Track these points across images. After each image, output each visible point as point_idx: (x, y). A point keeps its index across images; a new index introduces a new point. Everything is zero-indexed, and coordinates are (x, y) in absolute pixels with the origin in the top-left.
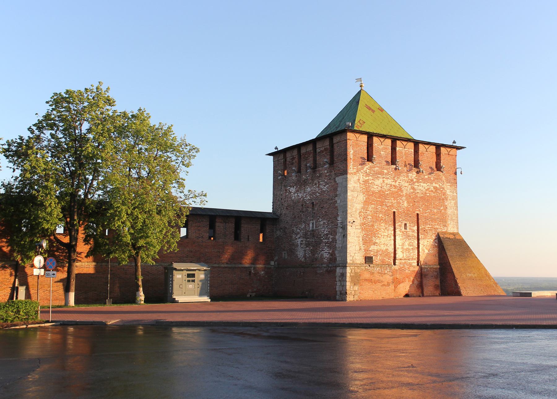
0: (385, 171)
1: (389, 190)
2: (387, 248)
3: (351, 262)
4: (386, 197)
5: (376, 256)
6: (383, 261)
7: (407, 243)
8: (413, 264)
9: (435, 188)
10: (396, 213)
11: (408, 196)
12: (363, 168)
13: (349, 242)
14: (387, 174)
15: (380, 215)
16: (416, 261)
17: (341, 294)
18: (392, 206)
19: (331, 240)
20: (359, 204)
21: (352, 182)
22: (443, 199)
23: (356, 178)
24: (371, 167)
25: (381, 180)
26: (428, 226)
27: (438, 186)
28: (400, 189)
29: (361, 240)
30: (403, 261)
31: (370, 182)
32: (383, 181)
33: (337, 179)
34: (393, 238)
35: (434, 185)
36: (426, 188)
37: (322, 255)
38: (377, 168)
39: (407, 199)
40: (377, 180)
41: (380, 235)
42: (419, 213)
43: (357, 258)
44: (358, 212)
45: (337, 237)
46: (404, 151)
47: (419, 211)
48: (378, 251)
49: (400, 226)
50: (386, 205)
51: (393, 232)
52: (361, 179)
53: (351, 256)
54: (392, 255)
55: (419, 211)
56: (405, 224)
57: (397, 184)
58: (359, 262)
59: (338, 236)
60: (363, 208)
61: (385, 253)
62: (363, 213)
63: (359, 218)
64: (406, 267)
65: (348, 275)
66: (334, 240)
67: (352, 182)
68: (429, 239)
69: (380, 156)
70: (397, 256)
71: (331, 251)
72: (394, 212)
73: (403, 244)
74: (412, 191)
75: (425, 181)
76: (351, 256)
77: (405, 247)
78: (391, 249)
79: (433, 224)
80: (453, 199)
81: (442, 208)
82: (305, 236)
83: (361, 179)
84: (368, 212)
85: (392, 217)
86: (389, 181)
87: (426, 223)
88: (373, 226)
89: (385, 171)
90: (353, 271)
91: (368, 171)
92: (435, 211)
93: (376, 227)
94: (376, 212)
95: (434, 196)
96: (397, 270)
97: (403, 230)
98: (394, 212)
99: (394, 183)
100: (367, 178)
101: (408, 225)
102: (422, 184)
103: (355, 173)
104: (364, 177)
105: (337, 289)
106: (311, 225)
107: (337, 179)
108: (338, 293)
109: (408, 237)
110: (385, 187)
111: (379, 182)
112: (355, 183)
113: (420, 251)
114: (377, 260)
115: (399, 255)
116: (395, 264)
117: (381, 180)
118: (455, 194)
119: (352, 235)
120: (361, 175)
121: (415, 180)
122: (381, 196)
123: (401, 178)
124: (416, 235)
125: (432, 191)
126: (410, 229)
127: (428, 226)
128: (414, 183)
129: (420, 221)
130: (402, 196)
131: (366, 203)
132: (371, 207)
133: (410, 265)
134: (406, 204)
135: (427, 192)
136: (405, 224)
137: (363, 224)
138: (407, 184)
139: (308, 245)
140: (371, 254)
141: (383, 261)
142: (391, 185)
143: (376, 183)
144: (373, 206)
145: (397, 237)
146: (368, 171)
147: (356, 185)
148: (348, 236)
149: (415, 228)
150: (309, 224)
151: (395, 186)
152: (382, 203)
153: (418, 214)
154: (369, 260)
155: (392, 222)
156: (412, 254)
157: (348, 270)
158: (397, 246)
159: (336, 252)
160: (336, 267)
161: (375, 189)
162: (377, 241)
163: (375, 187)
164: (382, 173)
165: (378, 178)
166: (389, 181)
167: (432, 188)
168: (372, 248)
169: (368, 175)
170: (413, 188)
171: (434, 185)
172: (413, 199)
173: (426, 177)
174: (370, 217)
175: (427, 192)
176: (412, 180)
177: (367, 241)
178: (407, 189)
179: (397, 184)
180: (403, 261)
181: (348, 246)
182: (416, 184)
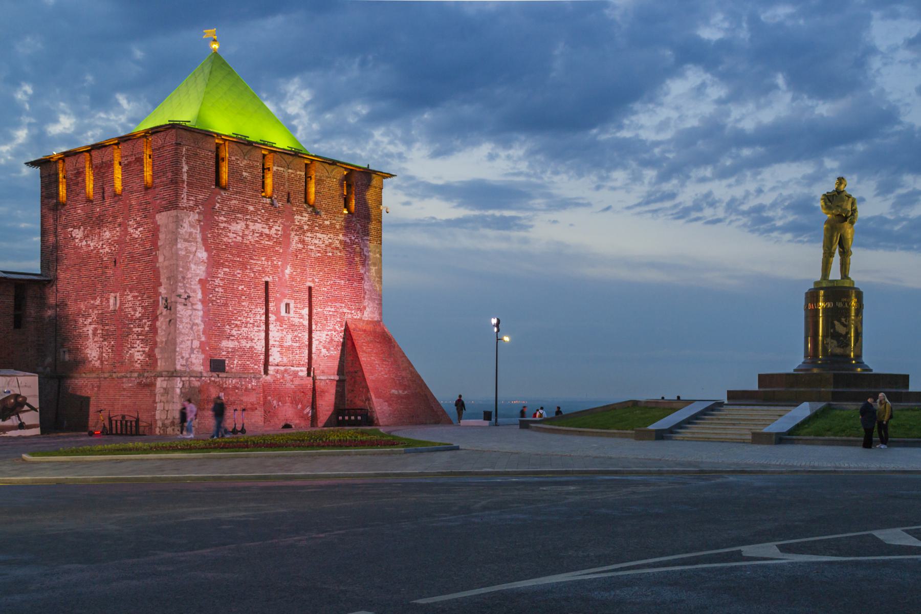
0: (251, 208)
3: (183, 369)
5: (232, 359)
6: (245, 367)
7: (289, 337)
8: (300, 374)
10: (271, 286)
13: (180, 333)
14: (252, 213)
16: (305, 369)
17: (163, 424)
19: (147, 329)
21: (184, 225)
30: (282, 368)
31: (222, 225)
32: (247, 226)
33: (158, 217)
34: (263, 327)
36: (327, 242)
37: (132, 356)
38: (234, 202)
40: (235, 224)
42: (312, 285)
43: (194, 361)
45: (158, 324)
51: (263, 318)
54: (262, 357)
55: (313, 281)
56: (287, 305)
59: (161, 323)
66: (154, 329)
68: (331, 330)
70: (271, 359)
71: (147, 349)
74: (300, 246)
75: (324, 229)
76: (183, 358)
78: (260, 347)
79: (338, 305)
80: (375, 264)
82: (101, 320)
86: (258, 227)
88: (226, 305)
89: (251, 208)
90: (187, 385)
99: (266, 231)
101: (292, 306)
102: (319, 235)
105: (157, 417)
106: (112, 301)
107: (158, 217)
108: (159, 423)
111: (238, 227)
112: (191, 226)
113: (314, 350)
114: (234, 364)
115: (275, 357)
116: (266, 372)
118: (378, 255)
121: (306, 227)
124: (306, 323)
125: (337, 248)
126: (295, 312)
128: (304, 232)
129: (314, 299)
133: (295, 374)
135: (329, 249)
136: (287, 305)
139: (105, 337)
142: (261, 234)
144: (227, 270)
145: (271, 327)
149: (306, 311)
150: (108, 300)
152: (243, 265)
153: (310, 288)
154: (217, 366)
158: (271, 342)
159: (157, 351)
160: (156, 377)
162: (234, 332)
163: (231, 235)
164: (245, 212)
165: (236, 220)
168: (225, 343)
173: (327, 223)
174: (220, 290)
176: (301, 228)
180: (282, 368)
181: (178, 340)
182: (309, 234)
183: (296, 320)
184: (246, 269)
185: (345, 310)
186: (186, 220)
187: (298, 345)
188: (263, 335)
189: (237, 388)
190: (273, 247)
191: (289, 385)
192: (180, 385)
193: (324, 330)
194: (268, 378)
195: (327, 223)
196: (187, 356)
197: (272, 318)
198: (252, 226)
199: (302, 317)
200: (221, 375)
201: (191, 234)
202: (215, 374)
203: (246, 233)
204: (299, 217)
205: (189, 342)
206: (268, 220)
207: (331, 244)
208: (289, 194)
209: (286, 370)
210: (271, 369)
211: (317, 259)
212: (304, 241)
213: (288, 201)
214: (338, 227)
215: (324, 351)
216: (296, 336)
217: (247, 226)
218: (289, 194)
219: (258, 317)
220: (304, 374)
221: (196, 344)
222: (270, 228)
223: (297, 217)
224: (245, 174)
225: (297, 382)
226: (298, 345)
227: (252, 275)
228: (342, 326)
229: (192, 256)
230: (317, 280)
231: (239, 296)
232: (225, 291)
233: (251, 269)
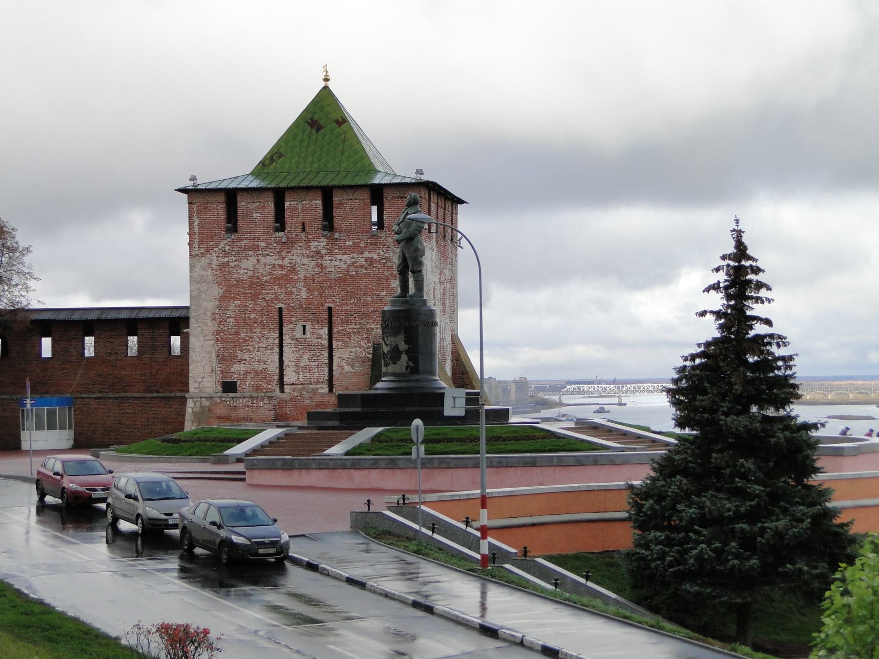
1: (270, 274)
2: (265, 366)
4: (262, 286)
5: (244, 380)
6: (257, 389)
7: (306, 357)
9: (370, 261)
10: (285, 311)
11: (309, 282)
12: (217, 245)
15: (252, 316)
18: (277, 299)
20: (211, 301)
22: (387, 279)
23: (204, 261)
24: (233, 241)
25: (253, 260)
26: (353, 326)
27: (375, 257)
28: (293, 270)
29: (214, 356)
30: (300, 387)
31: (232, 264)
32: (258, 261)
34: (277, 350)
35: (367, 254)
36: (349, 262)
39: (306, 285)
41: (251, 348)
43: (206, 384)
44: (209, 314)
46: (300, 206)
47: (334, 301)
48: (247, 372)
49: (292, 330)
50: (264, 299)
51: (277, 341)
52: (215, 262)
53: (196, 382)
54: (276, 377)
57: (286, 262)
58: (211, 391)
60: (219, 307)
61: (262, 374)
62: (220, 317)
63: (210, 324)
64: (306, 395)
65: (189, 410)
67: (197, 269)
69: (253, 221)
70: (286, 379)
72: (280, 309)
73: (298, 359)
74: (317, 270)
75: (345, 250)
76: (196, 382)
77: (302, 364)
78: (274, 368)
79: (363, 321)
81: (384, 293)
83: (215, 262)
84: (228, 313)
85: (277, 317)
86: (270, 260)
87: (346, 321)
88: (237, 333)
89: (263, 244)
90: (198, 404)
91: (227, 248)
92: (369, 299)
93: (243, 335)
94: (243, 312)
95: (367, 275)
96: (286, 401)
97: (299, 334)
98: (280, 309)
100: (226, 260)
101: (307, 328)
103: (203, 255)
104: (220, 259)
109: (309, 347)
110: (261, 271)
111: (249, 263)
112: (203, 269)
113: (334, 368)
114: (246, 387)
115: (290, 376)
116: (282, 390)
117: (253, 260)
119: (197, 350)
120: (214, 256)
121: (323, 252)
122: (255, 285)
123: (294, 251)
124: (326, 342)
125: (362, 266)
126: (313, 333)
127: (353, 326)
128: (322, 256)
130: (298, 280)
131: (224, 299)
132: (233, 305)
133: (315, 392)
134: (304, 293)
135: (352, 268)
136: (304, 327)
137: (218, 332)
138: (306, 261)
140: (235, 377)
141: (257, 389)
142: (274, 266)
143: (242, 265)
145: (285, 349)
146: (227, 248)
147: (205, 273)
148: (191, 352)
149: (325, 330)
151: (281, 266)
152: (255, 297)
153: (330, 309)
154: (229, 387)
155: (277, 325)
156: (316, 375)
157: (190, 404)
158: (286, 363)
161: (243, 275)
162: (246, 357)
163: (242, 271)
164: (255, 248)
165: (246, 257)
166: (270, 260)
167: (362, 261)
168: (236, 367)
169: (226, 254)
170: (322, 267)
171: (367, 254)
172: (319, 284)
173: (350, 243)
174: (232, 320)
175: (352, 268)
176: (318, 253)
177: (225, 359)
178: (306, 266)
179: (286, 262)
181: (191, 367)
182: (327, 258)
183: (314, 341)
184: (258, 298)
185: (373, 326)
186: (198, 265)
187: (316, 363)
188: (277, 357)
189: (248, 406)
190: (286, 275)
191: (307, 402)
192: (192, 405)
193: (347, 347)
194: (284, 396)
195: (348, 243)
196: (200, 380)
197: (287, 339)
198: (263, 260)
199: (320, 337)
200: (231, 395)
201: (202, 276)
202: (225, 395)
203: (257, 267)
204: (316, 243)
205: (201, 368)
206: (281, 251)
207: (353, 263)
208: (303, 224)
209: (304, 389)
210: (287, 389)
211: (339, 279)
212: (322, 265)
213: (304, 229)
214: (362, 245)
215: (347, 368)
216: (313, 355)
217: (258, 261)
218: (303, 224)
219: (271, 341)
220: (326, 390)
221: (208, 369)
222: (283, 259)
223: (313, 244)
224: (255, 215)
225: (317, 399)
226: (316, 363)
227: (265, 304)
228: (369, 342)
229: (203, 296)
230: (338, 300)
231: (250, 325)
232: (237, 321)
233: (264, 299)
